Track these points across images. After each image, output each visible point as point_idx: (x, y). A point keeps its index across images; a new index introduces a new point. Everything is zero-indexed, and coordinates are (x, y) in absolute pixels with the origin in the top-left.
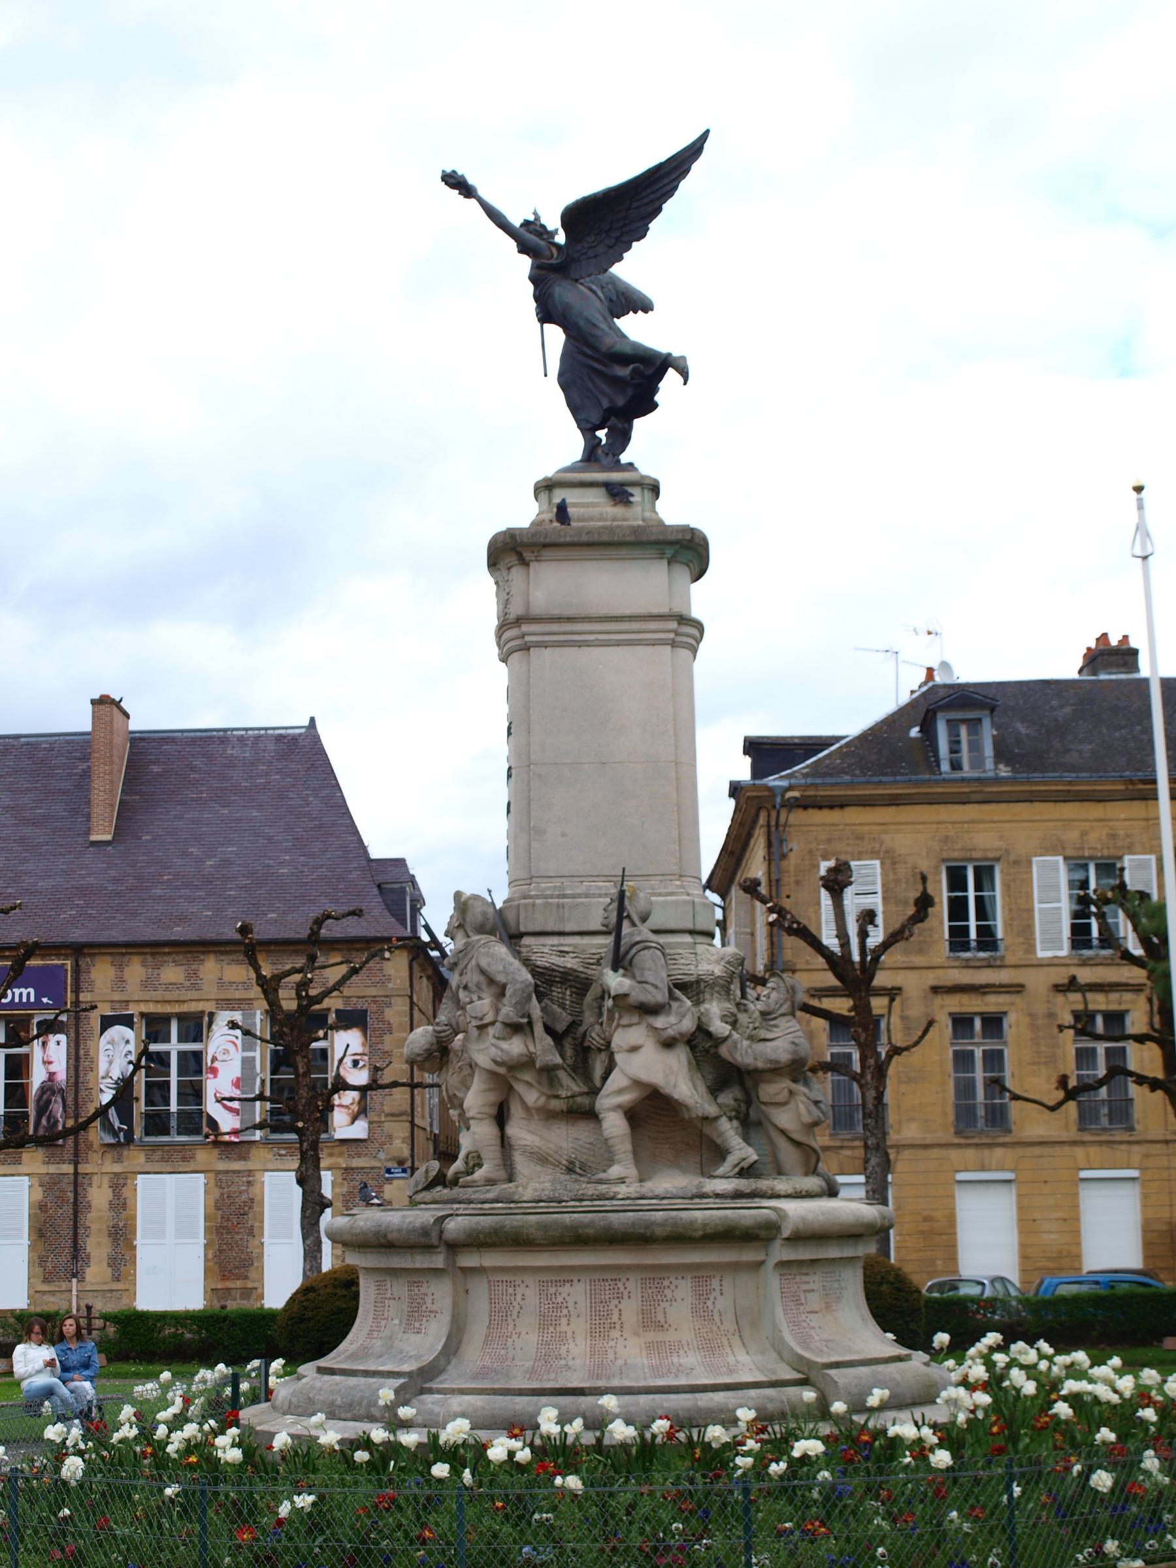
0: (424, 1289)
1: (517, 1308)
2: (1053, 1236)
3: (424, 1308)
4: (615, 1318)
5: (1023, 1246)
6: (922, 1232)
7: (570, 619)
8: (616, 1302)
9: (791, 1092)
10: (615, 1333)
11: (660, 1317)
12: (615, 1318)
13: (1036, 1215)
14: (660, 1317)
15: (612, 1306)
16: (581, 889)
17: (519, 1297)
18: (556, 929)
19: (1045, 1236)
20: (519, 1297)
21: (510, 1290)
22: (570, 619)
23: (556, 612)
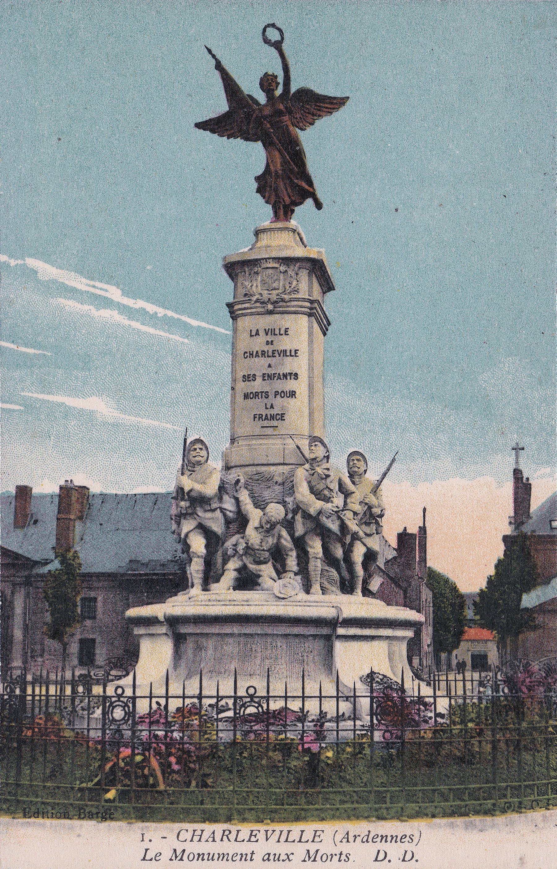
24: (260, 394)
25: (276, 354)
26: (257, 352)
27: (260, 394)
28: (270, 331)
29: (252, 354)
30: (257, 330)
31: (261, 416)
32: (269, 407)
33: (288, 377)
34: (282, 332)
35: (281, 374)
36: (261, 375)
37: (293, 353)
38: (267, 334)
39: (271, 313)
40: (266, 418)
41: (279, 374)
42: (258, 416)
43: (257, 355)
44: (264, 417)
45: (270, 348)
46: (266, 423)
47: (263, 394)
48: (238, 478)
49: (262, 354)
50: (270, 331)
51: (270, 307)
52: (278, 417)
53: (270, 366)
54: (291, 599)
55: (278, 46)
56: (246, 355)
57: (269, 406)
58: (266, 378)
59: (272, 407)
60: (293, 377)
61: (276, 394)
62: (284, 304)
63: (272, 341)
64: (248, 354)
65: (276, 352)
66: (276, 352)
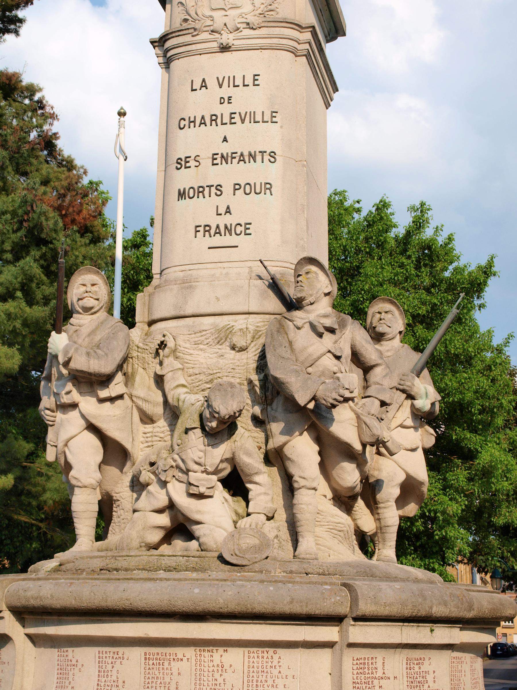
24: (207, 189)
25: (237, 119)
26: (203, 117)
27: (207, 189)
28: (226, 80)
29: (194, 122)
30: (204, 80)
31: (207, 228)
32: (223, 213)
33: (259, 158)
34: (249, 80)
35: (246, 154)
36: (211, 156)
37: (267, 118)
38: (221, 86)
40: (218, 232)
41: (242, 155)
42: (201, 229)
43: (203, 123)
44: (212, 232)
45: (226, 110)
46: (217, 240)
47: (213, 189)
48: (163, 339)
49: (212, 120)
50: (226, 80)
51: (227, 38)
52: (239, 229)
53: (225, 140)
54: (257, 567)
56: (183, 123)
57: (222, 210)
58: (218, 161)
59: (228, 211)
60: (266, 157)
61: (237, 187)
62: (252, 32)
63: (230, 98)
64: (187, 122)
65: (237, 116)
66: (237, 116)
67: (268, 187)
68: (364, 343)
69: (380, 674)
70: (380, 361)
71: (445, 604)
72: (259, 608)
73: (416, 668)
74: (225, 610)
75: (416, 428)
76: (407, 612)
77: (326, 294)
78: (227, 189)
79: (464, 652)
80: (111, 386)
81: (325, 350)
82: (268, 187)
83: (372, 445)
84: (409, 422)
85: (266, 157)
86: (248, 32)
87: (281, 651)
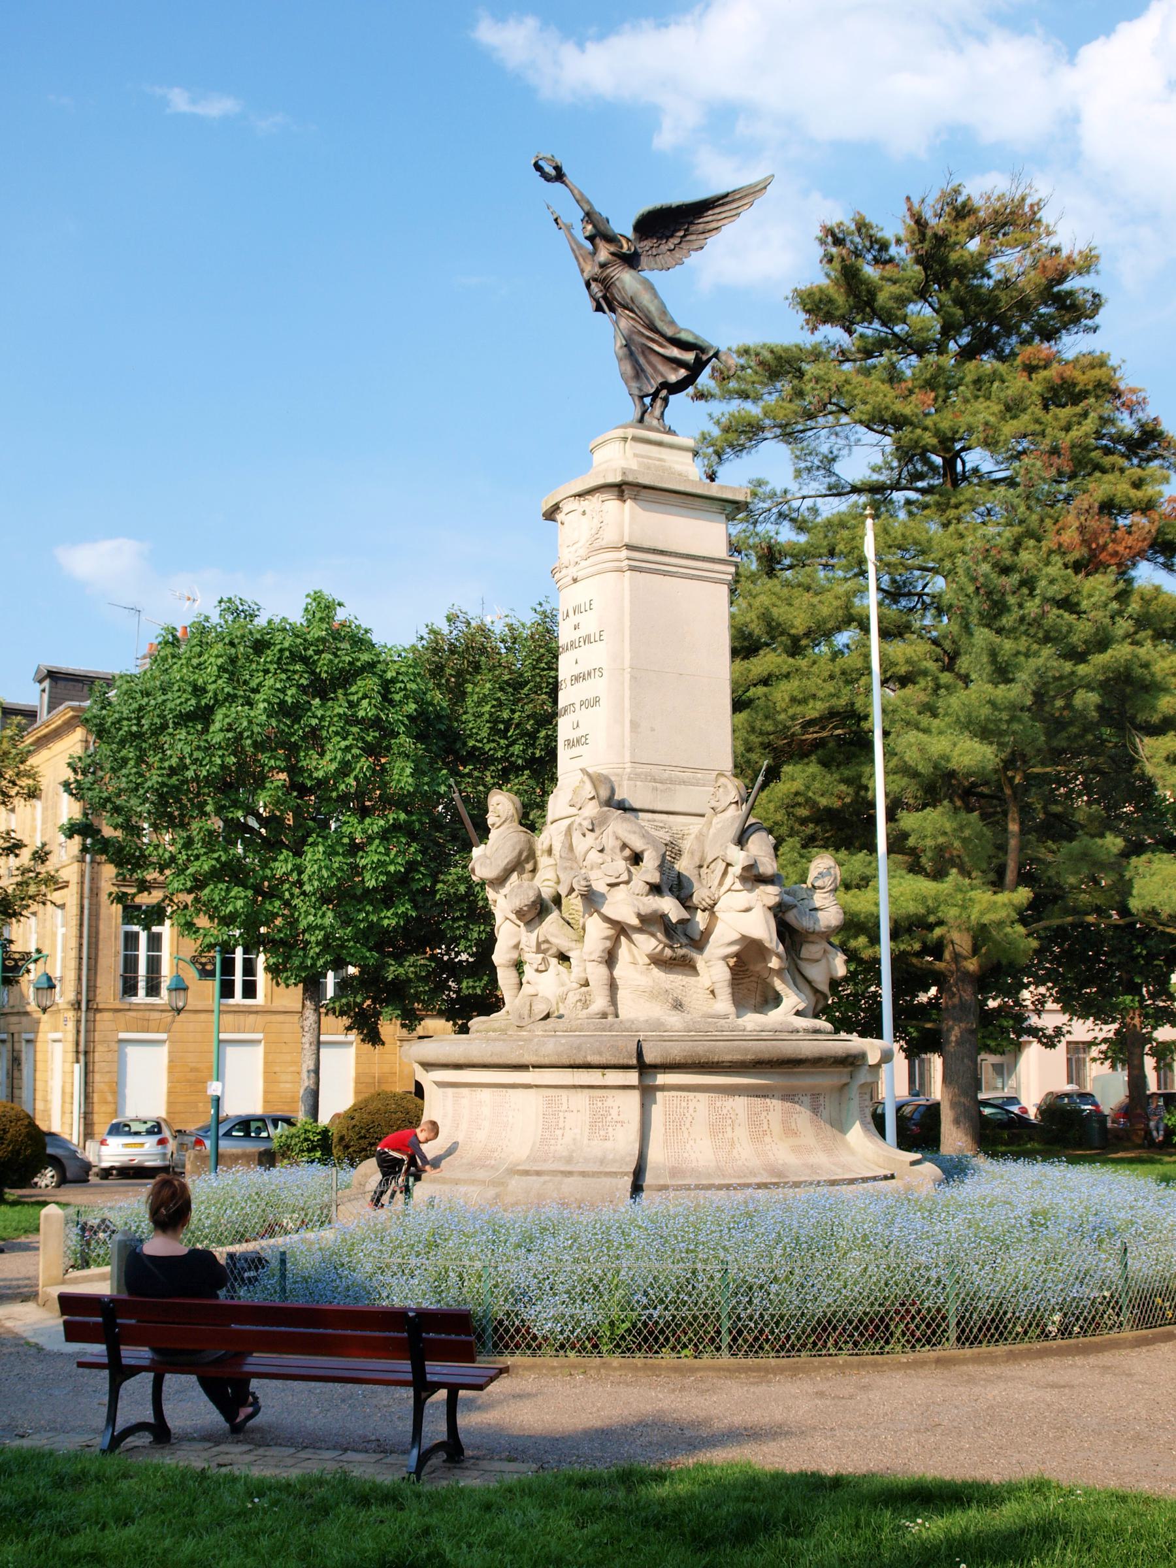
0: (609, 1102)
1: (690, 1119)
2: (288, 1085)
3: (609, 1118)
4: (765, 1127)
5: (266, 1092)
6: (189, 1081)
7: (662, 553)
8: (764, 1114)
9: (825, 951)
10: (767, 1139)
11: (794, 1126)
12: (765, 1127)
13: (277, 1069)
14: (794, 1126)
15: (762, 1117)
16: (666, 775)
17: (691, 1110)
18: (651, 808)
19: (282, 1085)
20: (691, 1110)
21: (684, 1104)
22: (662, 553)
23: (646, 544)
39: (575, 580)
45: (575, 635)
55: (559, 176)
60: (597, 673)
67: (597, 701)
68: (626, 834)
69: (565, 1107)
70: (644, 847)
71: (600, 1054)
72: (476, 1060)
73: (600, 1104)
74: (437, 1061)
75: (750, 890)
76: (566, 1061)
77: (593, 798)
78: (577, 706)
79: (689, 1091)
80: (508, 884)
81: (587, 846)
82: (597, 701)
83: (704, 911)
84: (738, 886)
85: (597, 673)
86: (583, 564)
87: (510, 1091)
